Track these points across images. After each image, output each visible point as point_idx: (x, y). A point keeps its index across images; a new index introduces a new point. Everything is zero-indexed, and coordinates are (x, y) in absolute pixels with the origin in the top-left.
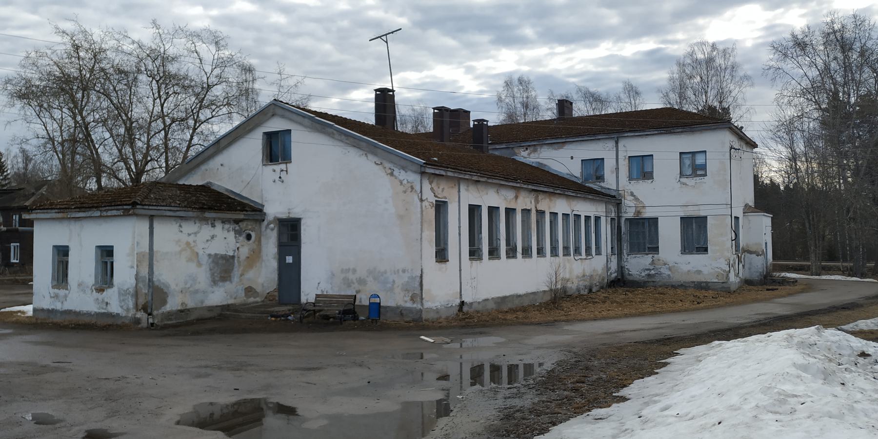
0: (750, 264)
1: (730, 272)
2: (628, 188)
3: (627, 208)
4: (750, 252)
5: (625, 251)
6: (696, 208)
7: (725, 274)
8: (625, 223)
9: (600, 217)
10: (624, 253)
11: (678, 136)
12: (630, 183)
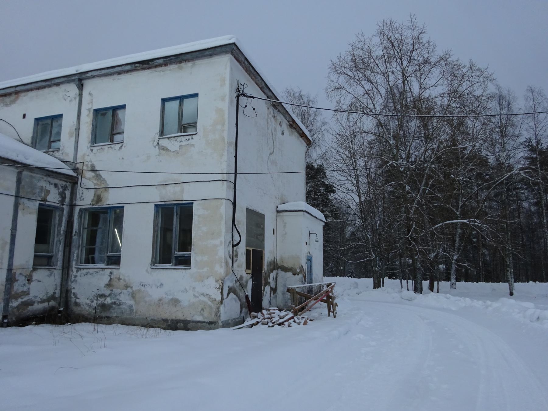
2: (87, 158)
3: (85, 190)
4: (285, 269)
6: (178, 188)
7: (214, 307)
8: (80, 216)
11: (162, 73)
12: (92, 150)
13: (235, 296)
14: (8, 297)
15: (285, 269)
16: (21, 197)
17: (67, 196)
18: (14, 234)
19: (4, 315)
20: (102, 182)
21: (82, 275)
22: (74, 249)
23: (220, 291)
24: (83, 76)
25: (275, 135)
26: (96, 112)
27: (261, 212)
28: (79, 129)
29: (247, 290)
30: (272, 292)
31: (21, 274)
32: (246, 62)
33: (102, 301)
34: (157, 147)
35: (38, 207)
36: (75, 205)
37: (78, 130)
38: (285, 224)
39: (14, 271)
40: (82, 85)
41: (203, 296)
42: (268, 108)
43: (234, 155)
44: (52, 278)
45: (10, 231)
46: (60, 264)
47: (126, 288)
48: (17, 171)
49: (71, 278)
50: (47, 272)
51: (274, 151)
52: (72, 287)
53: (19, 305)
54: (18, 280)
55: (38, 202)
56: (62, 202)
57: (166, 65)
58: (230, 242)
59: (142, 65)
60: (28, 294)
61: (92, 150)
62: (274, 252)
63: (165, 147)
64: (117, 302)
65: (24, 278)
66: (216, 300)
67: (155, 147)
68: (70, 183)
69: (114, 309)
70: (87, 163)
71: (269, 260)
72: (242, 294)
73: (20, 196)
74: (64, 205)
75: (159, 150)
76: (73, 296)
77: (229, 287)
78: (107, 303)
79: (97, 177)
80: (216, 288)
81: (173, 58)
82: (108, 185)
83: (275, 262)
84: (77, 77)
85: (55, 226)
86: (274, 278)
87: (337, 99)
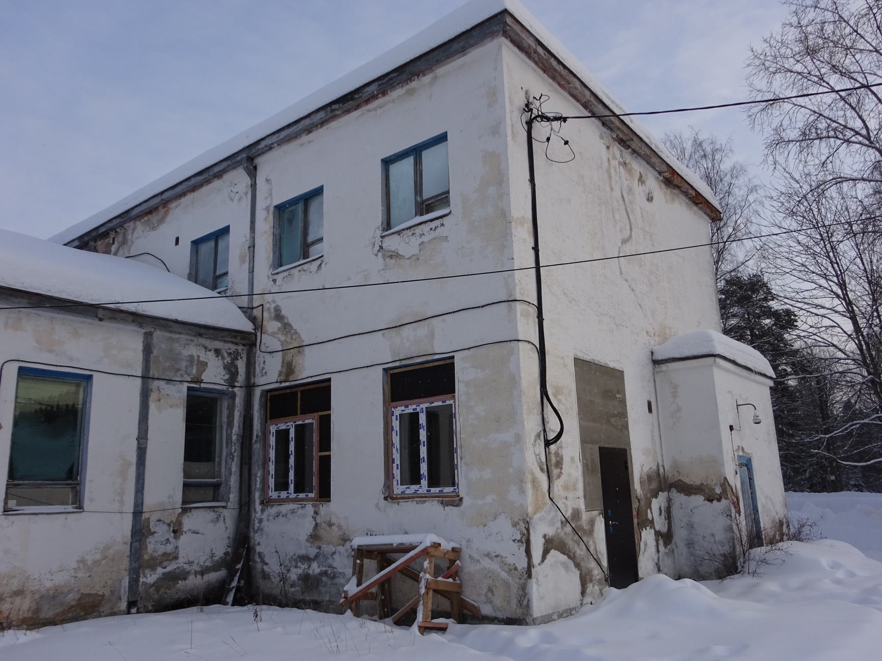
0: (690, 526)
1: (530, 576)
3: (267, 356)
4: (687, 489)
5: (257, 495)
6: (422, 330)
7: (514, 583)
9: (90, 377)
10: (254, 502)
12: (274, 281)
13: (563, 558)
14: (136, 565)
15: (687, 489)
16: (153, 379)
17: (239, 370)
18: (143, 446)
19: (131, 600)
20: (294, 337)
21: (271, 518)
22: (257, 468)
23: (523, 548)
24: (254, 151)
25: (631, 202)
26: (279, 210)
27: (612, 365)
28: (254, 246)
29: (594, 542)
30: (661, 542)
31: (159, 520)
32: (540, 50)
33: (304, 570)
34: (380, 254)
35: (185, 394)
36: (254, 386)
37: (252, 248)
38: (675, 387)
39: (145, 516)
40: (255, 168)
41: (489, 558)
42: (608, 147)
43: (532, 244)
44: (221, 524)
45: (136, 442)
46: (234, 497)
47: (342, 543)
48: (143, 331)
49: (254, 525)
50: (211, 515)
51: (631, 236)
52: (256, 542)
53: (158, 579)
54: (155, 532)
55: (186, 385)
56: (231, 382)
57: (384, 93)
58: (538, 436)
59: (343, 104)
60: (176, 558)
61: (274, 281)
62: (655, 451)
63: (394, 252)
64: (329, 572)
65: (166, 527)
66: (516, 569)
67: (376, 255)
68: (244, 345)
69: (324, 586)
70: (268, 305)
71: (646, 469)
72: (581, 550)
73: (151, 376)
74: (235, 387)
75: (384, 260)
76: (258, 560)
77: (545, 536)
78: (313, 573)
79: (285, 328)
80: (514, 541)
81: (395, 75)
82: (303, 341)
83: (661, 474)
84: (244, 155)
85: (221, 426)
86: (663, 509)
87: (774, 126)
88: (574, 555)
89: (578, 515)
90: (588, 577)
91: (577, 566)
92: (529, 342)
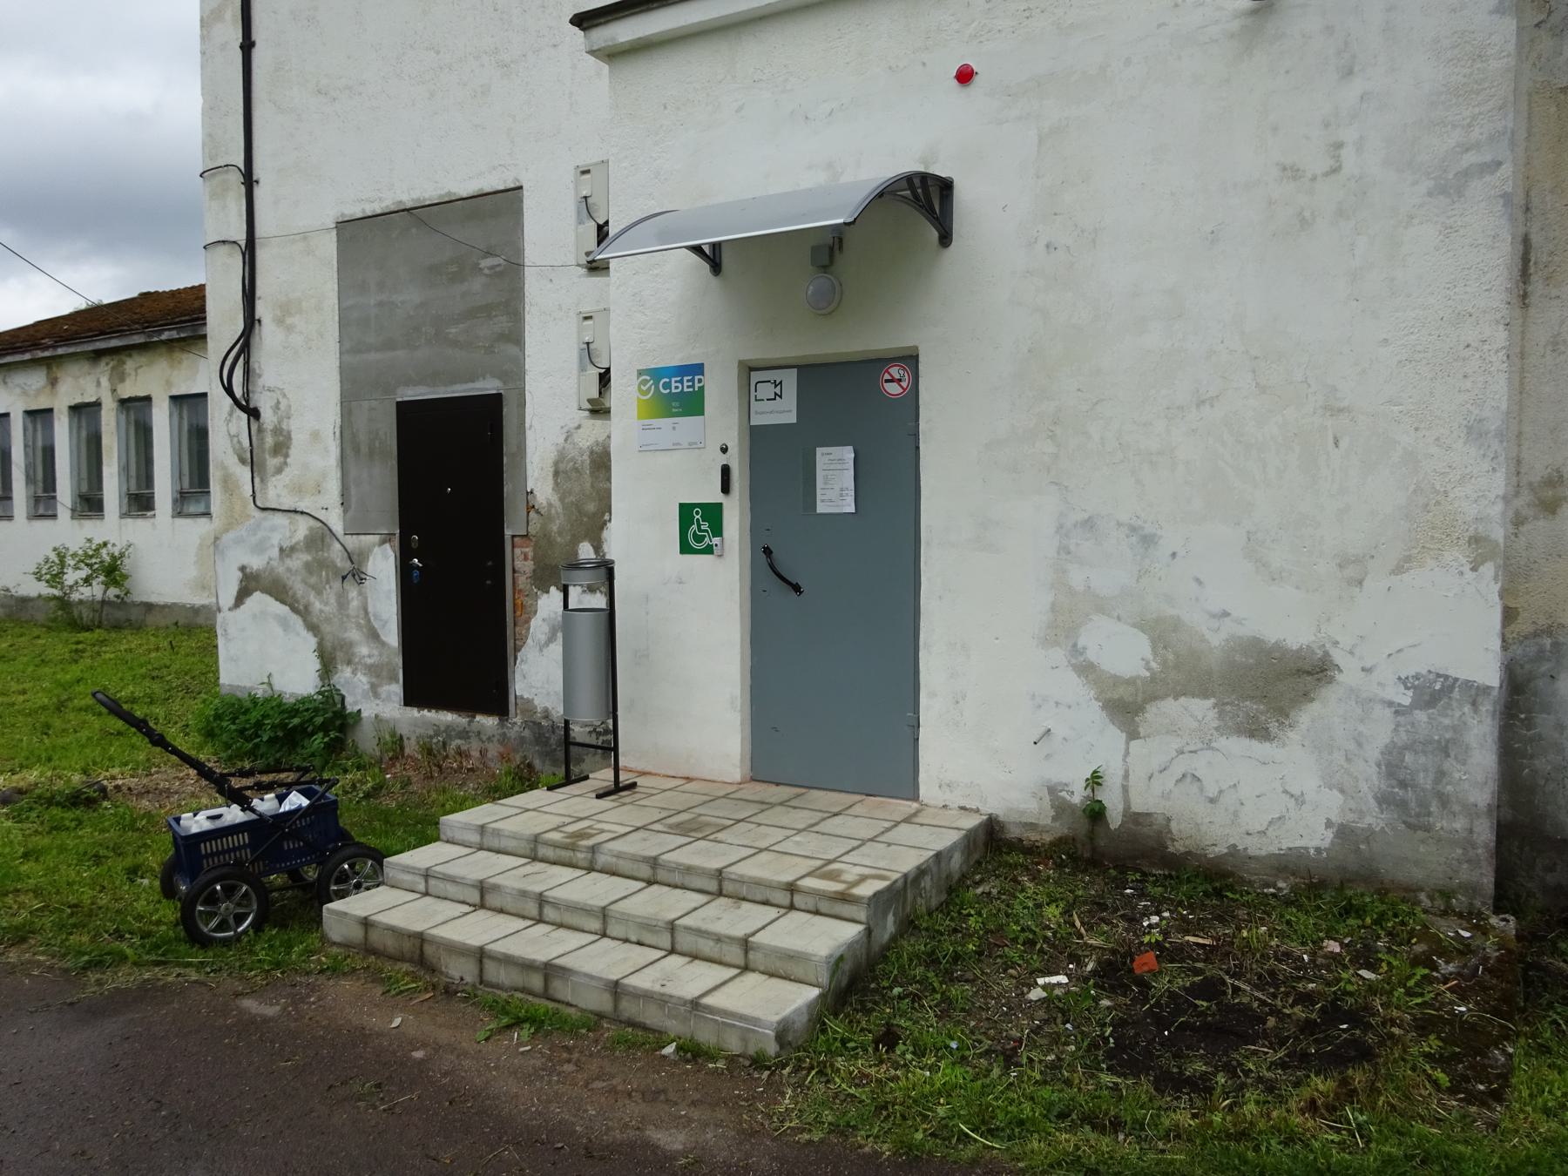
77: (243, 569)
88: (306, 607)
89: (323, 541)
90: (340, 655)
91: (313, 628)
92: (224, 242)
